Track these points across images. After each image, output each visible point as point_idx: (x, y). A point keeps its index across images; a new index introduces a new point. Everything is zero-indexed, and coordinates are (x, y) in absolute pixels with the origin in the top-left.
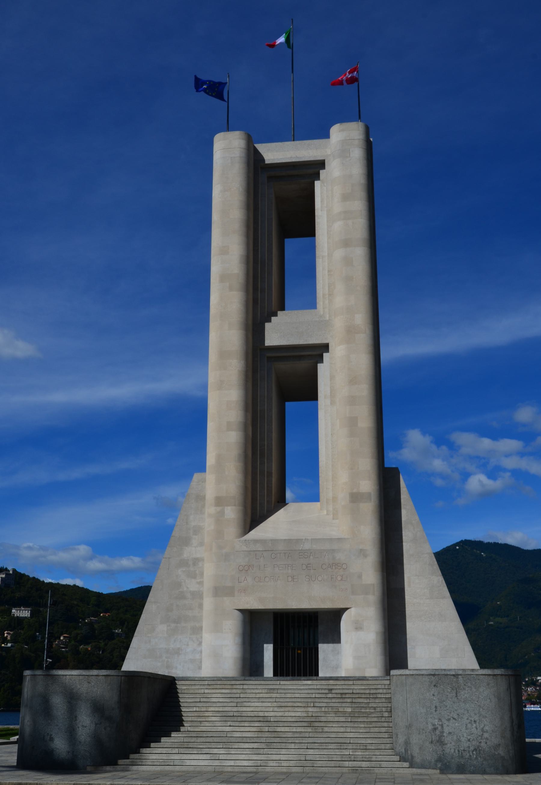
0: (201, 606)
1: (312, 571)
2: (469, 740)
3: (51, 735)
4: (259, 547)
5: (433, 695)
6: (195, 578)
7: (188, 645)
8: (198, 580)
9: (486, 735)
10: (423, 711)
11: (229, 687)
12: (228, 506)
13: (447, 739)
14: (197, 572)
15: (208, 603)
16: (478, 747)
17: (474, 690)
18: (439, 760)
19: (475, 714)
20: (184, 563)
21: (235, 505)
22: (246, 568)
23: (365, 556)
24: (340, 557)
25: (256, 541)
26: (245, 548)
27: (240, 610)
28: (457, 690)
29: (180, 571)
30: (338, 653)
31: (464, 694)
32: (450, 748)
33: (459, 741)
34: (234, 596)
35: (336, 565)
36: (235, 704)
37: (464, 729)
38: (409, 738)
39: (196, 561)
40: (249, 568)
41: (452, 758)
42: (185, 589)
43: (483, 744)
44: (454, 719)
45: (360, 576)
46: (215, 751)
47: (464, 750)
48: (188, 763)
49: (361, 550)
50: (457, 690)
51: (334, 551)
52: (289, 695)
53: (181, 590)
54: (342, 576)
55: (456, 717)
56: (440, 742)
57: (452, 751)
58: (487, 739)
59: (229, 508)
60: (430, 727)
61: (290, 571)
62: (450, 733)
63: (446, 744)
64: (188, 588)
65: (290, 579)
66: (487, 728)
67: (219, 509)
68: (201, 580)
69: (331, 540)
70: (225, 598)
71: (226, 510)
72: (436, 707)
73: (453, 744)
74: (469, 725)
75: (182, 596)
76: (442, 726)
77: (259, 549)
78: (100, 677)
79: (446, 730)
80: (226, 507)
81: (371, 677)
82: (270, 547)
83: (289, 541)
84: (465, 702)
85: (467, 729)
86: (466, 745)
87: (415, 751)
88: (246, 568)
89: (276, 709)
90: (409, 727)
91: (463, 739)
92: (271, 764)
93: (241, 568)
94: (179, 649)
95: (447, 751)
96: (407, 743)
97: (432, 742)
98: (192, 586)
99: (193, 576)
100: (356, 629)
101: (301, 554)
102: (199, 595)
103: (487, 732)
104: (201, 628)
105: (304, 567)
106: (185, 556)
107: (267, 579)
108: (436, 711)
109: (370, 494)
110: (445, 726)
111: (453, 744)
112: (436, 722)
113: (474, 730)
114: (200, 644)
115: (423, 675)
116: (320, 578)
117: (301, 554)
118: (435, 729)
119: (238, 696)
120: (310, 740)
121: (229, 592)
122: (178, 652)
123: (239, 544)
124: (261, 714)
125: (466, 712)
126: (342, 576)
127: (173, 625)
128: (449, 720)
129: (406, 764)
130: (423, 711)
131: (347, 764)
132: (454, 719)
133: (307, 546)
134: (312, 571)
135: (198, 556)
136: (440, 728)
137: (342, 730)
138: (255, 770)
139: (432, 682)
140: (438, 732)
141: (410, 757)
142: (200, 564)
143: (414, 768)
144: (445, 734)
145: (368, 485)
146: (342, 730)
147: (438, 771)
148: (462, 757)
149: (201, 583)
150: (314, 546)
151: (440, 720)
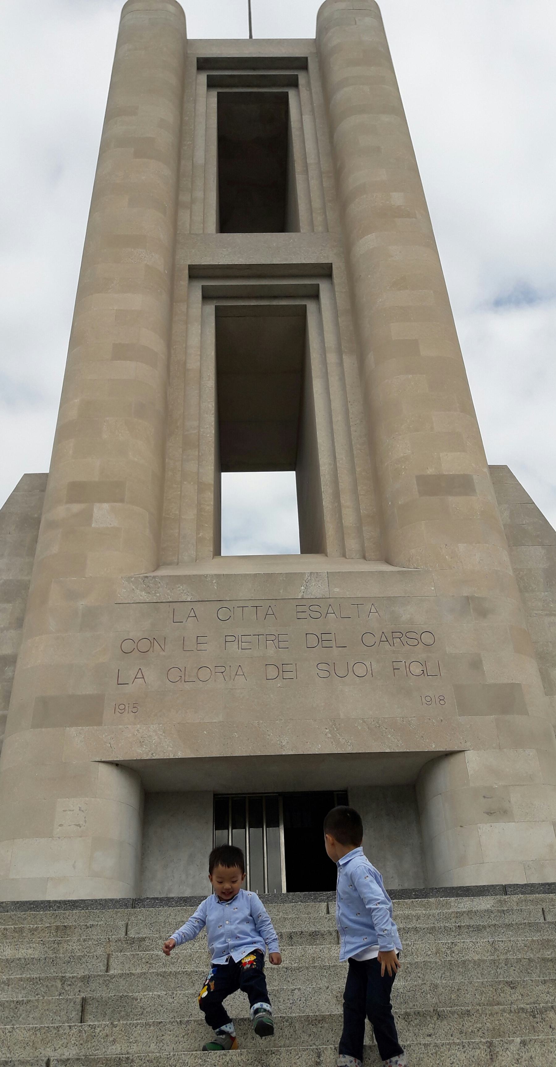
12: (101, 501)
26: (143, 596)
27: (117, 764)
34: (100, 724)
35: (401, 635)
40: (152, 645)
49: (467, 599)
54: (424, 664)
59: (106, 506)
61: (271, 651)
65: (272, 672)
67: (76, 508)
70: (72, 731)
71: (95, 510)
77: (184, 598)
88: (144, 645)
93: (127, 646)
100: (490, 813)
101: (300, 608)
105: (313, 640)
107: (204, 674)
116: (360, 670)
117: (300, 608)
121: (88, 711)
126: (424, 664)
133: (317, 590)
134: (335, 651)
150: (337, 590)
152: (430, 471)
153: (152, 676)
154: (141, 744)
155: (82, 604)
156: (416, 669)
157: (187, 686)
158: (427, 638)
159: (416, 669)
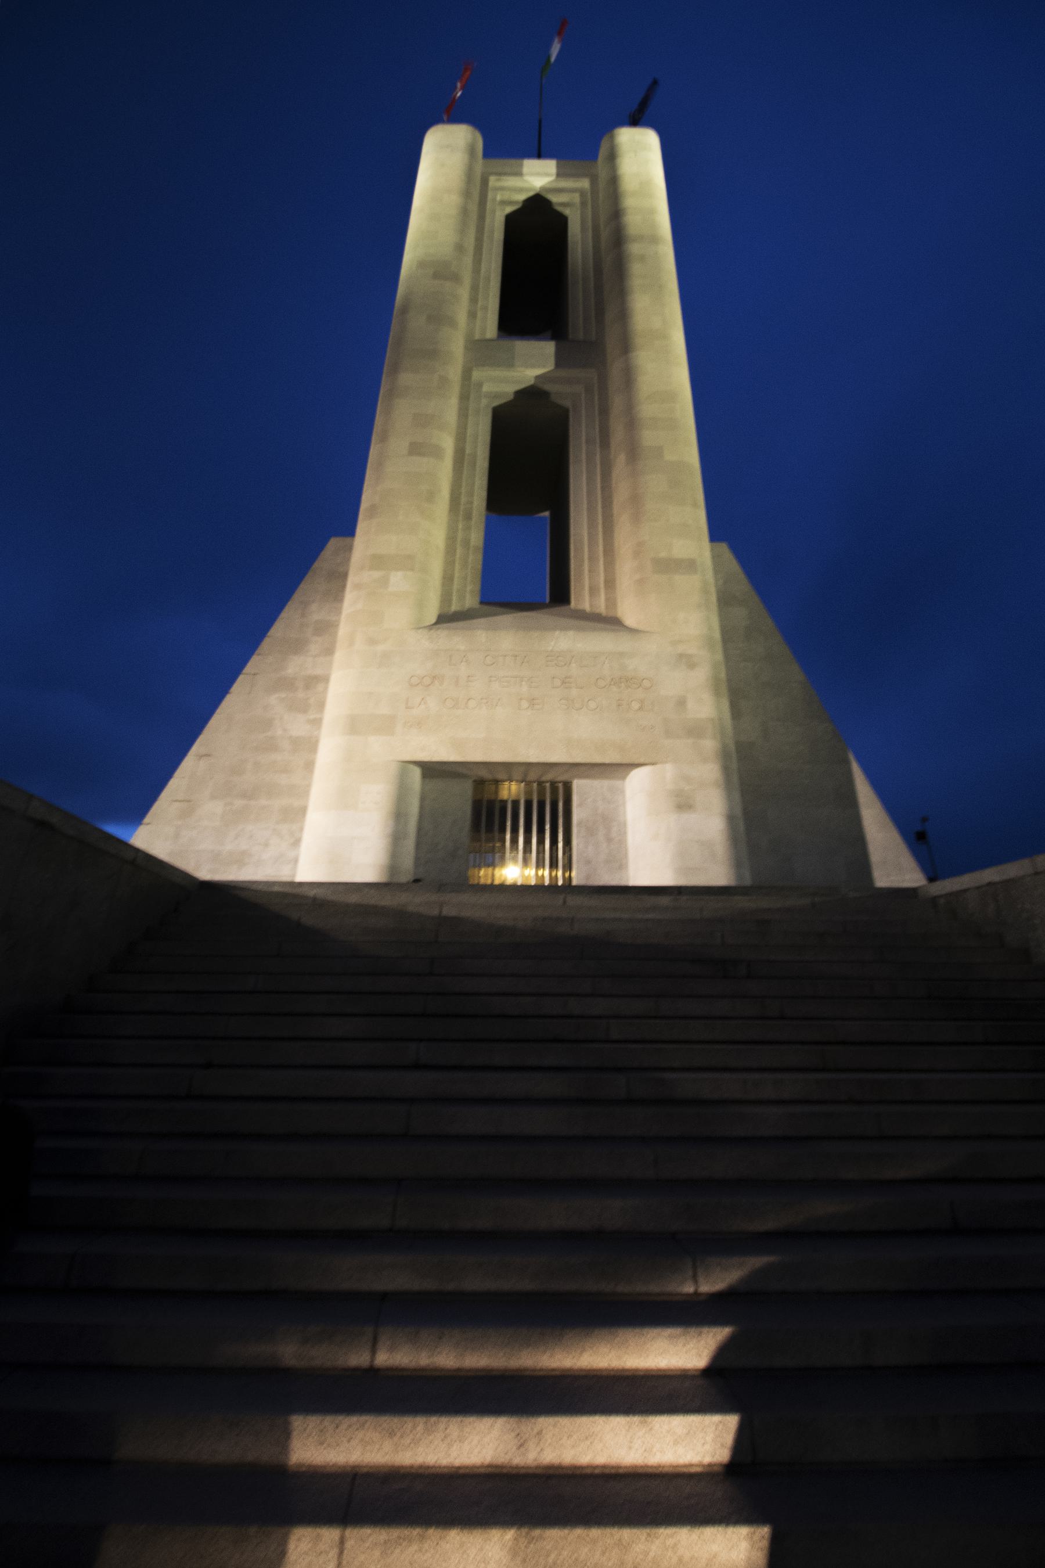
0: (310, 766)
1: (574, 692)
8: (312, 717)
15: (330, 748)
35: (626, 681)
42: (280, 732)
49: (681, 656)
51: (621, 654)
53: (269, 734)
54: (642, 701)
64: (285, 730)
68: (318, 716)
75: (271, 746)
104: (303, 810)
114: (297, 843)
116: (592, 705)
126: (642, 701)
127: (239, 803)
135: (319, 671)
142: (320, 687)
149: (317, 723)
152: (663, 554)
156: (636, 705)
158: (646, 683)
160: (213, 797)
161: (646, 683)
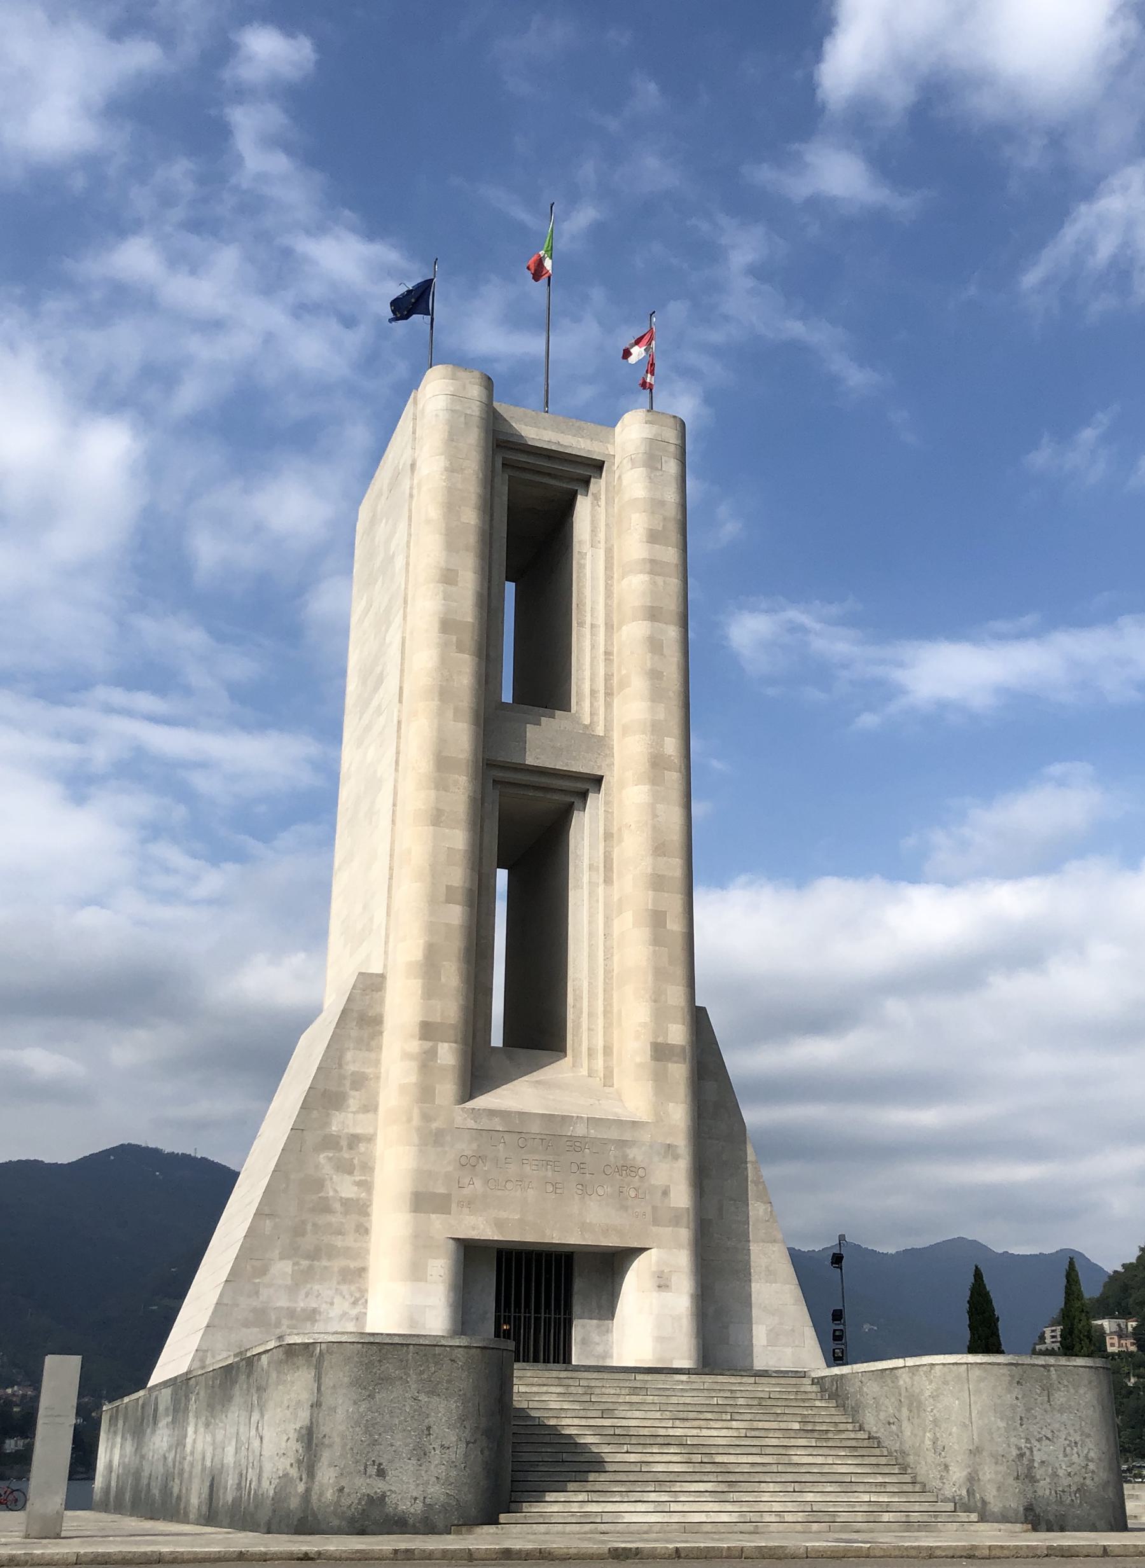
0: (363, 1230)
2: (1069, 1474)
3: (380, 1464)
4: (497, 1124)
5: (1017, 1398)
6: (351, 1173)
7: (332, 1304)
8: (357, 1179)
9: (1092, 1466)
10: (1002, 1424)
11: (556, 1382)
13: (1039, 1473)
14: (356, 1161)
16: (1083, 1485)
17: (1072, 1391)
18: (1029, 1509)
19: (1075, 1431)
20: (330, 1143)
21: (456, 1042)
22: (473, 1161)
23: (676, 1157)
24: (636, 1154)
25: (492, 1113)
26: (471, 1124)
28: (1048, 1390)
29: (322, 1158)
30: (609, 1331)
31: (1060, 1398)
32: (1044, 1488)
33: (1055, 1475)
35: (627, 1169)
36: (599, 1414)
37: (1061, 1456)
38: (976, 1472)
39: (355, 1140)
41: (1048, 1505)
42: (331, 1193)
43: (1088, 1482)
44: (1047, 1438)
45: (666, 1193)
46: (653, 1497)
47: (1063, 1491)
48: (628, 1518)
50: (1048, 1390)
52: (674, 1400)
55: (1049, 1435)
56: (1029, 1477)
57: (1047, 1492)
58: (1093, 1472)
59: (446, 1045)
60: (1015, 1452)
61: (550, 1173)
62: (1043, 1462)
63: (1038, 1481)
64: (336, 1191)
65: (550, 1188)
66: (1092, 1454)
69: (620, 1123)
70: (433, 1216)
72: (1021, 1419)
73: (1048, 1480)
74: (1068, 1449)
75: (324, 1207)
76: (1031, 1449)
78: (456, 1350)
79: (1038, 1457)
80: (440, 1044)
81: (776, 1372)
82: (515, 1126)
83: (549, 1118)
84: (1061, 1411)
85: (1066, 1455)
86: (1065, 1482)
87: (990, 1494)
88: (473, 1161)
89: (678, 1423)
90: (976, 1452)
91: (1061, 1473)
92: (768, 1518)
94: (314, 1311)
95: (1040, 1493)
96: (972, 1479)
97: (1017, 1478)
98: (345, 1187)
99: (346, 1168)
100: (659, 1287)
101: (569, 1143)
102: (360, 1209)
103: (1092, 1460)
105: (574, 1168)
106: (333, 1128)
108: (1021, 1425)
109: (683, 1048)
110: (1035, 1449)
111: (1048, 1480)
112: (1022, 1443)
113: (1075, 1458)
115: (999, 1364)
117: (569, 1143)
118: (1021, 1455)
119: (587, 1398)
120: (790, 1478)
122: (312, 1315)
123: (461, 1115)
124: (662, 1432)
125: (1063, 1428)
127: (305, 1263)
128: (1039, 1440)
129: (974, 1517)
130: (1002, 1424)
131: (886, 1517)
132: (1047, 1438)
133: (580, 1130)
135: (359, 1130)
136: (1028, 1453)
137: (820, 1460)
138: (752, 1529)
139: (1012, 1376)
140: (1025, 1461)
141: (979, 1504)
142: (362, 1147)
143: (987, 1521)
144: (1036, 1465)
145: (678, 1034)
146: (820, 1460)
147: (1030, 1526)
148: (1061, 1502)
151: (1028, 1440)
152: (660, 1040)
153: (478, 1183)
154: (474, 1228)
155: (434, 1125)
156: (633, 1193)
157: (499, 1193)
159: (633, 1193)
160: (281, 1259)
161: (641, 1172)
